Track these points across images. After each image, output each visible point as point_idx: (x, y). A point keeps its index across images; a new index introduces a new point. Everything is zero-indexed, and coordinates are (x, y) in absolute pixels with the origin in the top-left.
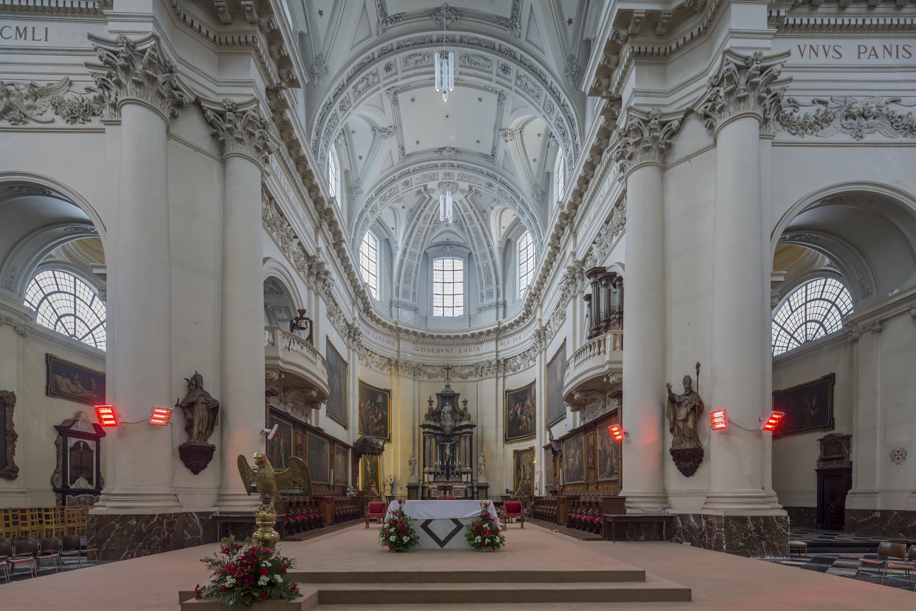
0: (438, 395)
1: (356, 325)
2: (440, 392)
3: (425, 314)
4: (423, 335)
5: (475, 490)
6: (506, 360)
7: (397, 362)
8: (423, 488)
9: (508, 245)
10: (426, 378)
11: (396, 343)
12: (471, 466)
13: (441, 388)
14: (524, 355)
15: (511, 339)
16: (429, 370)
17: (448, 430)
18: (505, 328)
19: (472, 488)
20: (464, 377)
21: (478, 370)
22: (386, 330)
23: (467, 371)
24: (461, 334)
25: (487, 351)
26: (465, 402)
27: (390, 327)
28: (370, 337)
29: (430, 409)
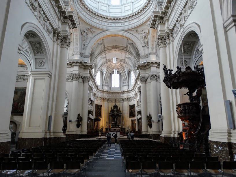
0: (113, 106)
1: (92, 86)
2: (113, 105)
3: (110, 86)
4: (110, 92)
5: (122, 129)
6: (129, 98)
7: (103, 98)
8: (109, 129)
9: (129, 73)
10: (110, 102)
11: (103, 94)
12: (121, 124)
13: (114, 104)
14: (133, 97)
15: (130, 93)
16: (111, 100)
17: (115, 114)
18: (129, 91)
19: (121, 129)
20: (119, 101)
21: (123, 100)
22: (101, 92)
23: (120, 100)
24: (119, 92)
25: (125, 96)
26: (120, 108)
27: (102, 91)
28: (99, 94)
29: (111, 110)
